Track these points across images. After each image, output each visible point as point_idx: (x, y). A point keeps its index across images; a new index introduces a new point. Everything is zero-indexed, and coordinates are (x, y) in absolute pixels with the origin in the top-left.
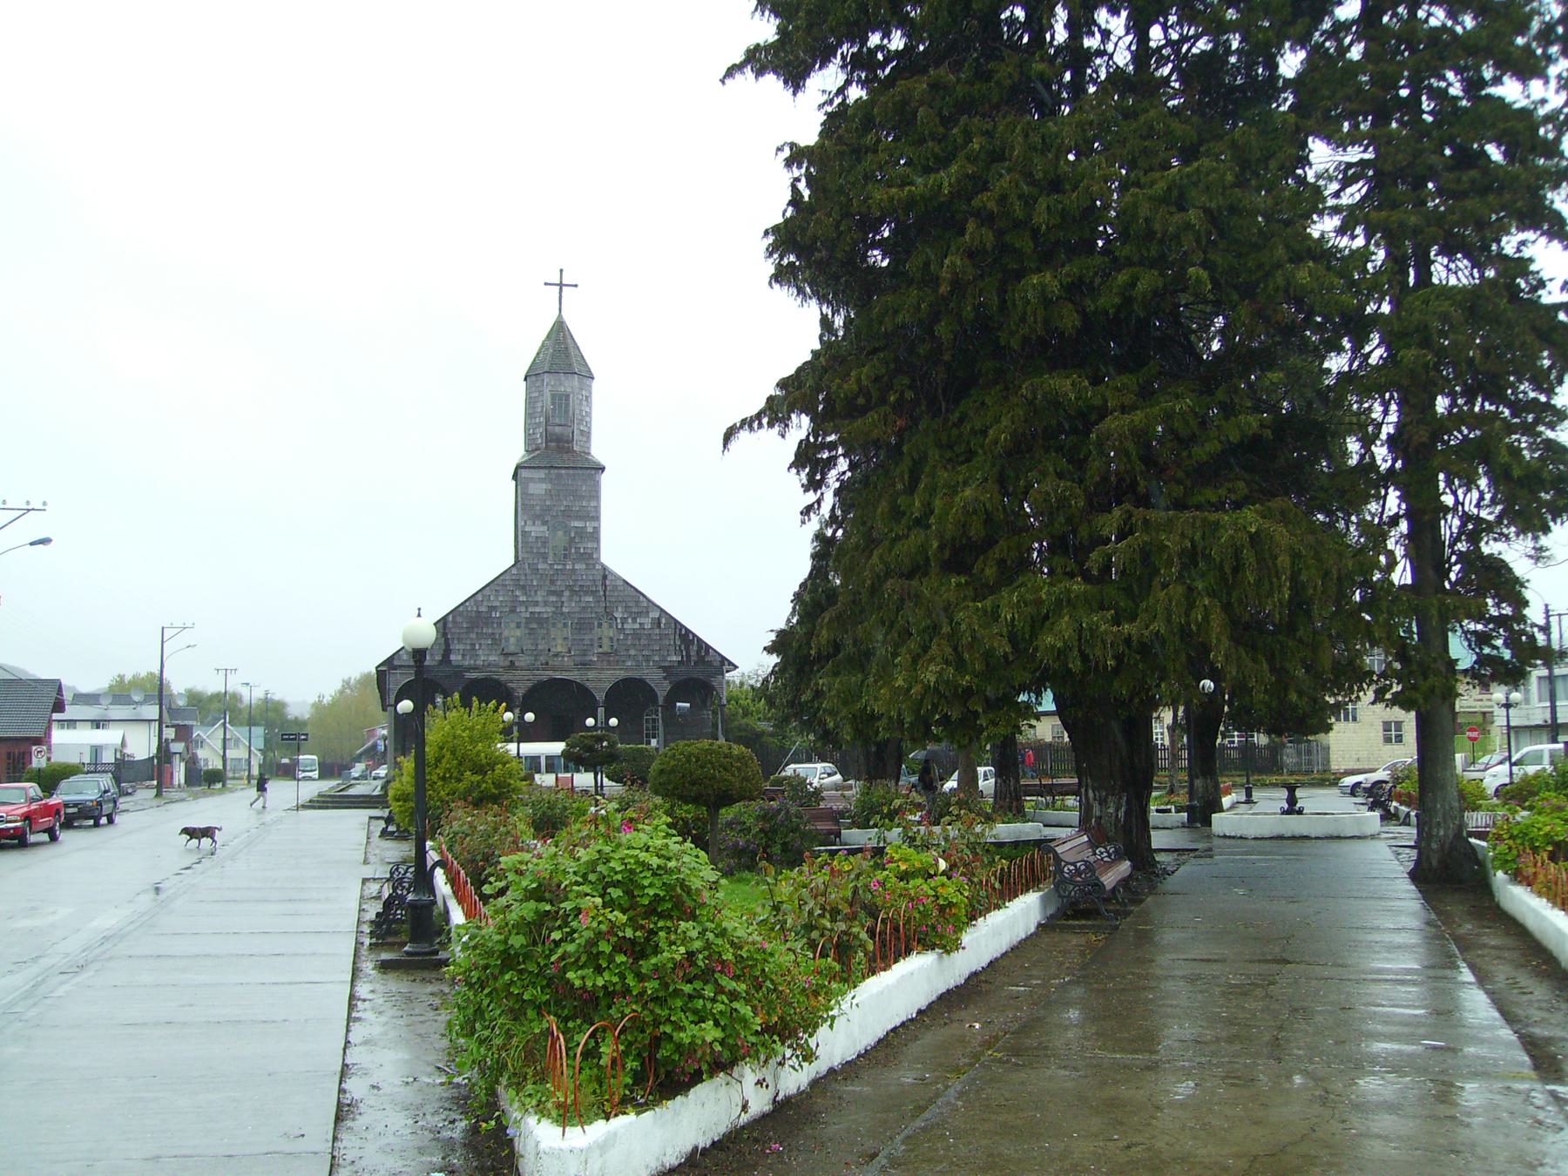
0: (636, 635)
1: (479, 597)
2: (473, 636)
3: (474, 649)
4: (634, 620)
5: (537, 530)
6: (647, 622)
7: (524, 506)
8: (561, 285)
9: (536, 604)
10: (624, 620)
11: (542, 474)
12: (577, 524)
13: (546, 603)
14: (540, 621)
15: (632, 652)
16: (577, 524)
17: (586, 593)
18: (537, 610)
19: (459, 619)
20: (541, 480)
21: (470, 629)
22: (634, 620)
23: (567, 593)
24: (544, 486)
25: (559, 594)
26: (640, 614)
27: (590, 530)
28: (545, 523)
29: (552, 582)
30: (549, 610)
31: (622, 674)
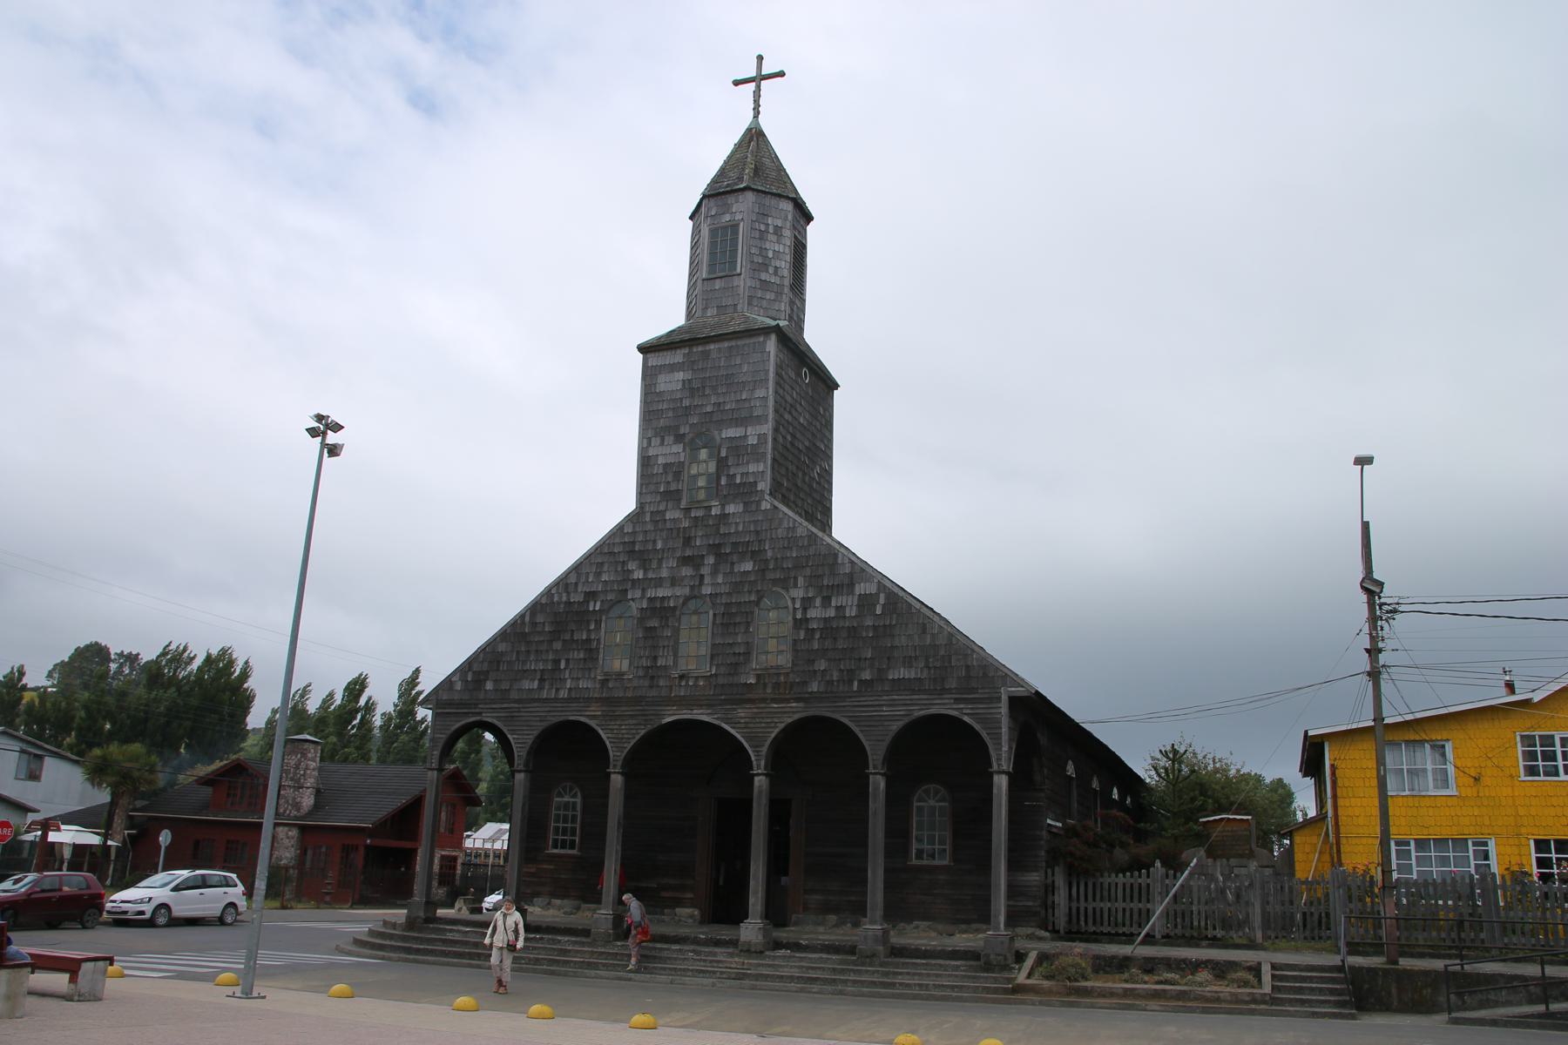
0: (829, 629)
1: (573, 579)
2: (558, 645)
3: (557, 669)
4: (826, 601)
5: (672, 451)
6: (850, 604)
7: (657, 416)
8: (759, 79)
9: (659, 582)
10: (807, 603)
11: (677, 357)
12: (731, 432)
13: (674, 582)
14: (660, 610)
15: (822, 665)
16: (731, 432)
17: (743, 556)
18: (661, 593)
19: (540, 619)
20: (673, 368)
21: (555, 635)
22: (826, 601)
23: (711, 560)
24: (680, 376)
25: (694, 561)
26: (838, 589)
27: (752, 440)
28: (679, 438)
29: (688, 541)
30: (679, 591)
31: (795, 712)
